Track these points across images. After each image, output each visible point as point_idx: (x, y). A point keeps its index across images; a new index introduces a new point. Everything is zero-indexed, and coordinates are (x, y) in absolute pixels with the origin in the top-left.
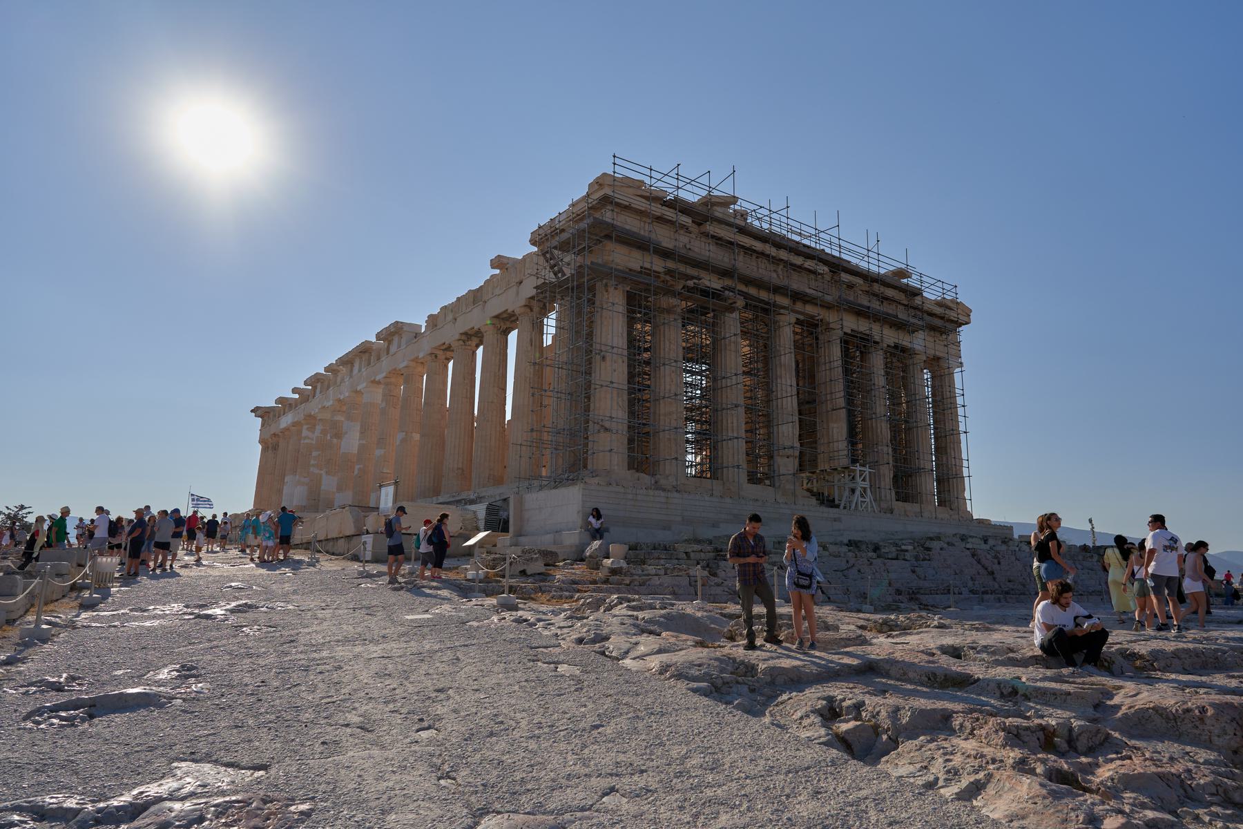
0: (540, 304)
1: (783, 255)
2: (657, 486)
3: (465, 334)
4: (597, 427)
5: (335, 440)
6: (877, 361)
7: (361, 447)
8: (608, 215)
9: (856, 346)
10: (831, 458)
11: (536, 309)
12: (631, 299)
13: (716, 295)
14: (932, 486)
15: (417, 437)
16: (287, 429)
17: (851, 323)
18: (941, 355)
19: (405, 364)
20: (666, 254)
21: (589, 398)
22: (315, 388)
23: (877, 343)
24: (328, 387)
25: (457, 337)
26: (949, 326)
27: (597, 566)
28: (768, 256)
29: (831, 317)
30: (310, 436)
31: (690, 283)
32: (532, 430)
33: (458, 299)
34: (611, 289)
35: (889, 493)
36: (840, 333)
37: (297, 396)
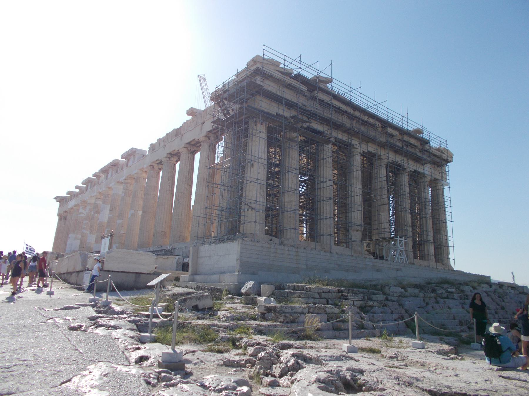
0: (214, 136)
1: (357, 114)
2: (282, 244)
3: (170, 154)
4: (247, 207)
5: (96, 215)
6: (405, 179)
7: (110, 218)
8: (259, 80)
9: (395, 169)
10: (380, 233)
11: (212, 138)
12: (270, 131)
13: (320, 133)
14: (432, 250)
15: (140, 213)
16: (72, 209)
17: (393, 157)
18: (437, 177)
19: (136, 171)
20: (290, 105)
21: (242, 189)
22: (87, 186)
23: (405, 169)
24: (95, 185)
25: (165, 155)
26: (443, 162)
27: (253, 302)
28: (349, 114)
29: (382, 152)
30: (84, 212)
31: (305, 125)
32: (207, 208)
33: (167, 134)
34: (259, 125)
35: (411, 255)
36: (386, 161)
37: (77, 190)
